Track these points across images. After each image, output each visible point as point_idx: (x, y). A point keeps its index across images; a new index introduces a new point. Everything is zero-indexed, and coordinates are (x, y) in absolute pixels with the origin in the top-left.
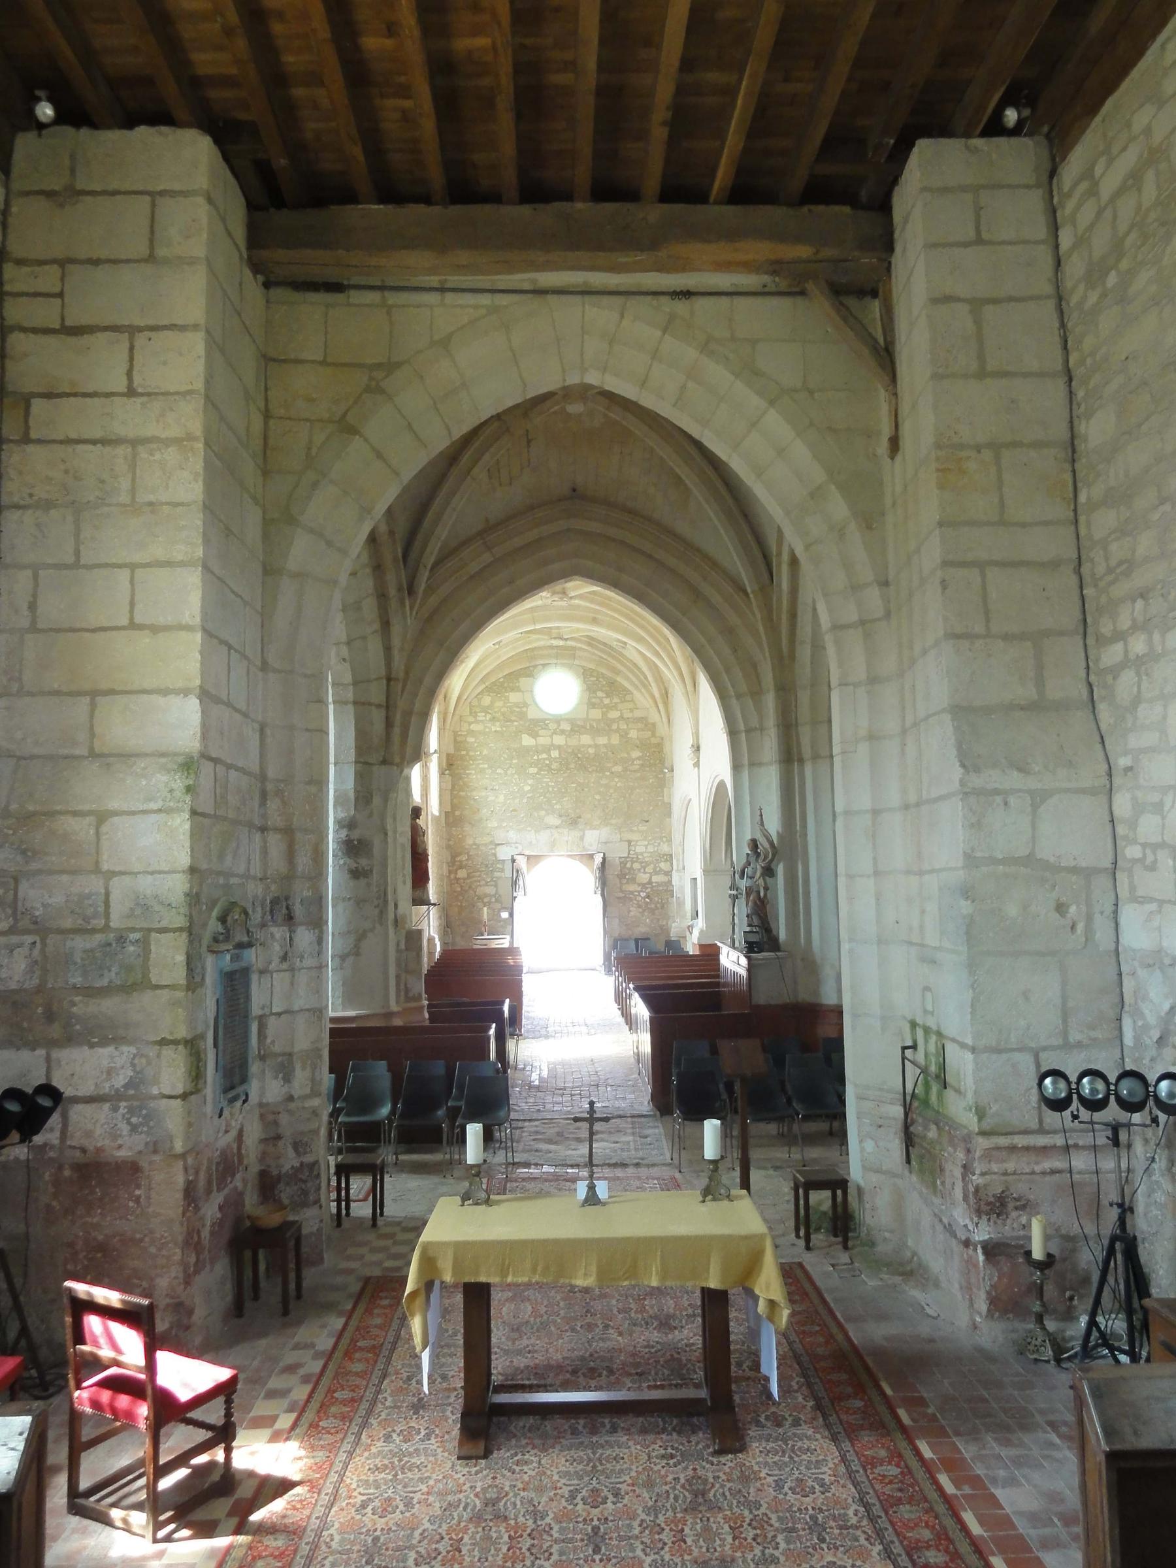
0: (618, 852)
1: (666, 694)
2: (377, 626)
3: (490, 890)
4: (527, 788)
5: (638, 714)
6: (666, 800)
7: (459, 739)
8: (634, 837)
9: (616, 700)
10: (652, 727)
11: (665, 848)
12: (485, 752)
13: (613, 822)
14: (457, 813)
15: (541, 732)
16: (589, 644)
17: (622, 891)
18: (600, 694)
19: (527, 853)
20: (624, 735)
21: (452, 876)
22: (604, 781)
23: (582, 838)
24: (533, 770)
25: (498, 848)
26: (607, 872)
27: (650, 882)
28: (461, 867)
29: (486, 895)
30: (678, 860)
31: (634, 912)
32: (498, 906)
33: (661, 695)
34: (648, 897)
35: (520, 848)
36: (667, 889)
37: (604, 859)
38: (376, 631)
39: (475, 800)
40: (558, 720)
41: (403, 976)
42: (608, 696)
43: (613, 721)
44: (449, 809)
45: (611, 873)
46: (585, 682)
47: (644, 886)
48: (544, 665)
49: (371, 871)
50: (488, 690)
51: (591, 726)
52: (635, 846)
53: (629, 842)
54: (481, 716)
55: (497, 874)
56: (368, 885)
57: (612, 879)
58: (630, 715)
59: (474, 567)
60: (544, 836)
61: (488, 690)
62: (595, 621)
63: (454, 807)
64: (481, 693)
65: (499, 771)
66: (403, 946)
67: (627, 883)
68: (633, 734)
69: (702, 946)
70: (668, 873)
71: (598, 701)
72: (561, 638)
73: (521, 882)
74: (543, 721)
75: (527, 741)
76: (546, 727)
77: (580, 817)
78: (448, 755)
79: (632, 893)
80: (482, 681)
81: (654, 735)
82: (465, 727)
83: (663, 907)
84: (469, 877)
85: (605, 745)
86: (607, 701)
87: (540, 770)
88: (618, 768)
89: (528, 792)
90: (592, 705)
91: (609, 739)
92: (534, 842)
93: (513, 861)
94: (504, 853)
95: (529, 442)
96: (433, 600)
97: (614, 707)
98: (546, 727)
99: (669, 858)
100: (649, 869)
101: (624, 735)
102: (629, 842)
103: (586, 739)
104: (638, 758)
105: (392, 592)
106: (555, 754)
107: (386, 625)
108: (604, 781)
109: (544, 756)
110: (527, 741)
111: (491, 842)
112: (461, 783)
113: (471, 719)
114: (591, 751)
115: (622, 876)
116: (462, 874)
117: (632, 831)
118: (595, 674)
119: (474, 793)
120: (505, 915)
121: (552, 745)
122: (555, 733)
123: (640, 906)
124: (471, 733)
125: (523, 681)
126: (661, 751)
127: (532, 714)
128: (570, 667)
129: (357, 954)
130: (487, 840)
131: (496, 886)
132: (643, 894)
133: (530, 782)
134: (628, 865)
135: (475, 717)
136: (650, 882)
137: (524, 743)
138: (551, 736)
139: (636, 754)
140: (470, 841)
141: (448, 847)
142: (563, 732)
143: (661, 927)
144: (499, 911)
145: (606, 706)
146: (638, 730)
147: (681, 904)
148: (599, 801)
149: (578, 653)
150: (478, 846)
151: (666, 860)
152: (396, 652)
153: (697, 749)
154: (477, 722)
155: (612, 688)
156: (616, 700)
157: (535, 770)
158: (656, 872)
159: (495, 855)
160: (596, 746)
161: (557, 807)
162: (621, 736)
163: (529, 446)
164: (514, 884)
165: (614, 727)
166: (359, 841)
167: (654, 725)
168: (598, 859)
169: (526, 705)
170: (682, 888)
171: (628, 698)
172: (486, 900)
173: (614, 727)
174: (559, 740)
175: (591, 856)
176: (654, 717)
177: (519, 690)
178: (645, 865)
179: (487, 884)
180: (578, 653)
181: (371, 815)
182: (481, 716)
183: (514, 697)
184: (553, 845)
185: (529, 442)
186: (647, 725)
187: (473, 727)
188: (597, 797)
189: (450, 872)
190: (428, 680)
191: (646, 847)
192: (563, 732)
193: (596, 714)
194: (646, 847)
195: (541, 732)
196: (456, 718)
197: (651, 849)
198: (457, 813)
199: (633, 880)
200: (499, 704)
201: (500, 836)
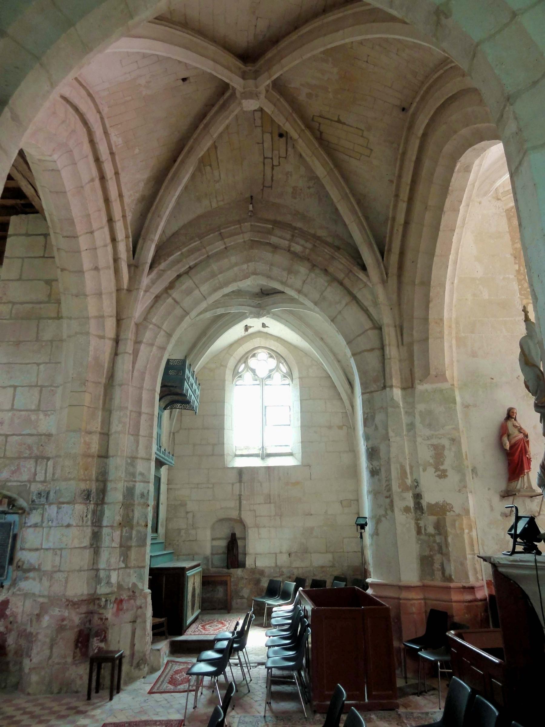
2: (347, 299)
38: (346, 305)
41: (438, 558)
49: (380, 469)
56: (379, 480)
59: (401, 218)
66: (431, 530)
95: (339, 121)
96: (394, 258)
105: (341, 276)
107: (354, 298)
129: (377, 534)
152: (371, 310)
163: (344, 124)
166: (372, 449)
181: (376, 428)
185: (339, 121)
190: (417, 313)
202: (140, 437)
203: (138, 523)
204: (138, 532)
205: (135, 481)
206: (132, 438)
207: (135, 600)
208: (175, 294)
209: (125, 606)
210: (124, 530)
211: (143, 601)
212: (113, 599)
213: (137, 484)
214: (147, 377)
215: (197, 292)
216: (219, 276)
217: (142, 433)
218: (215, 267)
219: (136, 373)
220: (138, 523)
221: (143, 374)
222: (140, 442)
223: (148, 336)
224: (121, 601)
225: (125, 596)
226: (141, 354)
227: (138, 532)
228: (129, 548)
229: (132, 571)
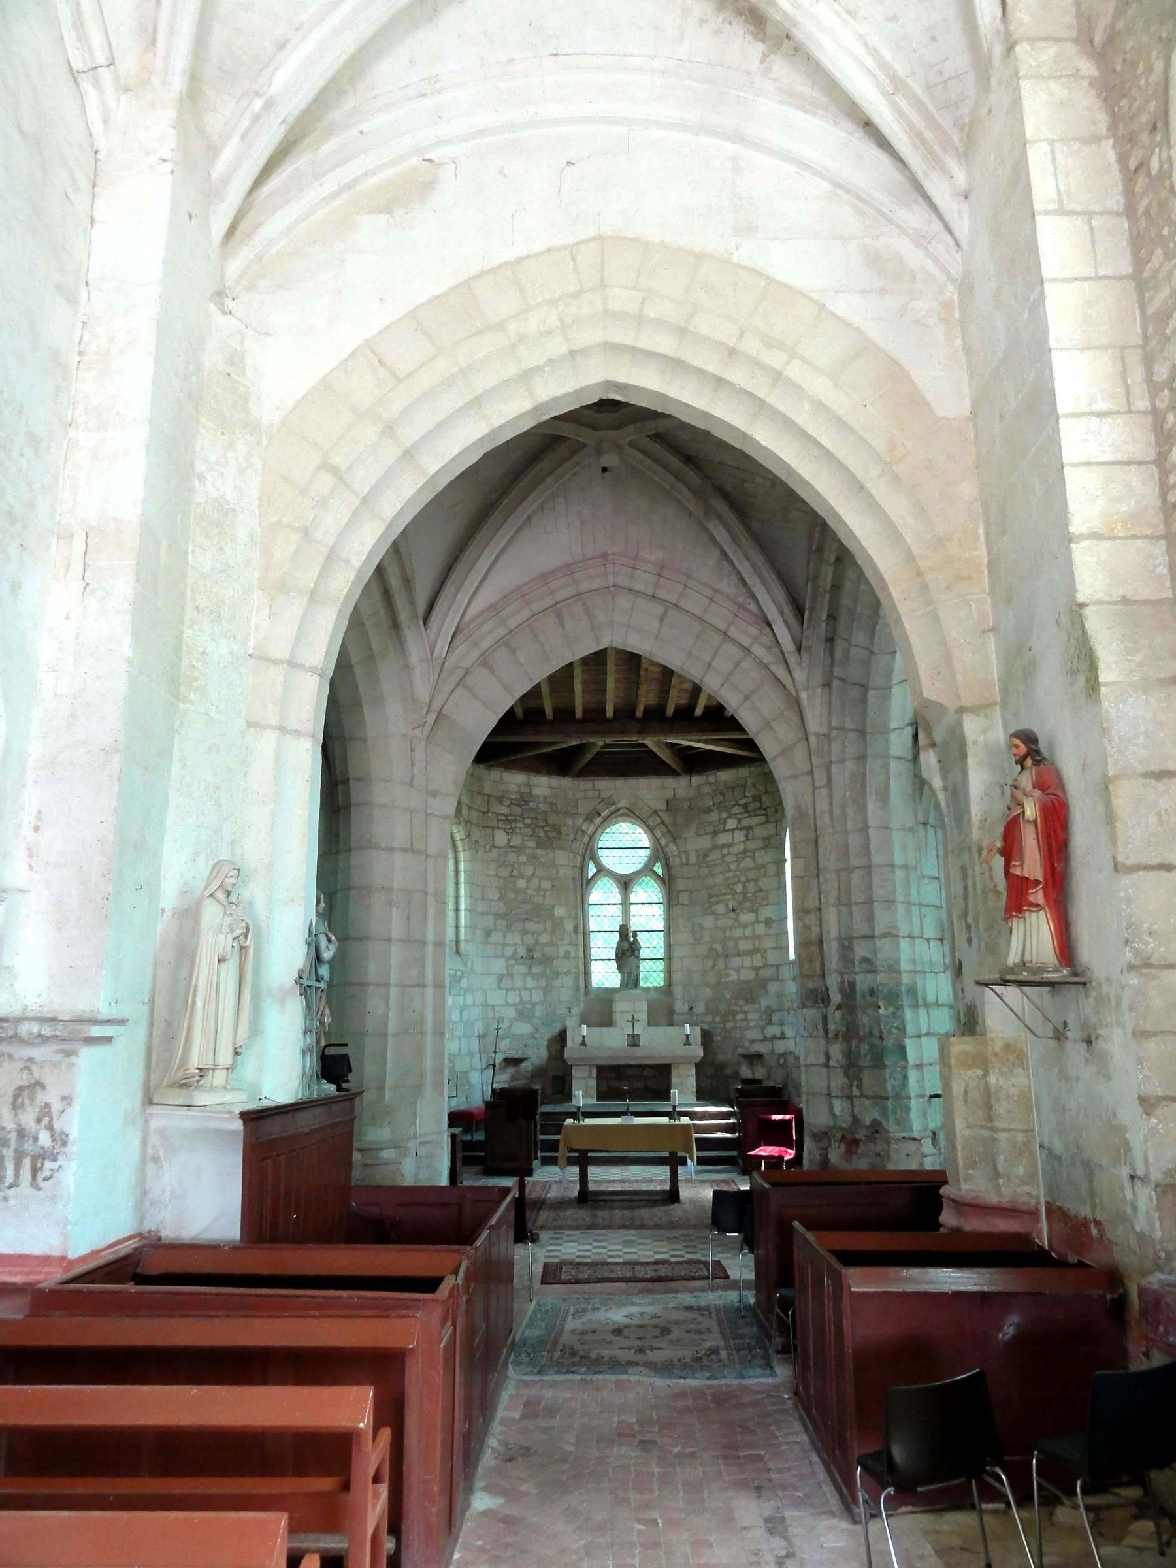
202: (854, 908)
203: (871, 1033)
204: (872, 1046)
205: (856, 973)
206: (844, 910)
207: (875, 1143)
208: (837, 671)
209: (862, 1148)
210: (854, 1043)
211: (886, 1147)
212: (839, 1135)
213: (859, 978)
214: (850, 812)
215: (854, 652)
216: (858, 611)
217: (857, 896)
218: (845, 601)
219: (837, 811)
220: (871, 1033)
221: (843, 807)
222: (855, 913)
223: (836, 748)
224: (856, 1142)
225: (861, 1135)
226: (834, 780)
227: (872, 1046)
228: (861, 1068)
229: (867, 1102)
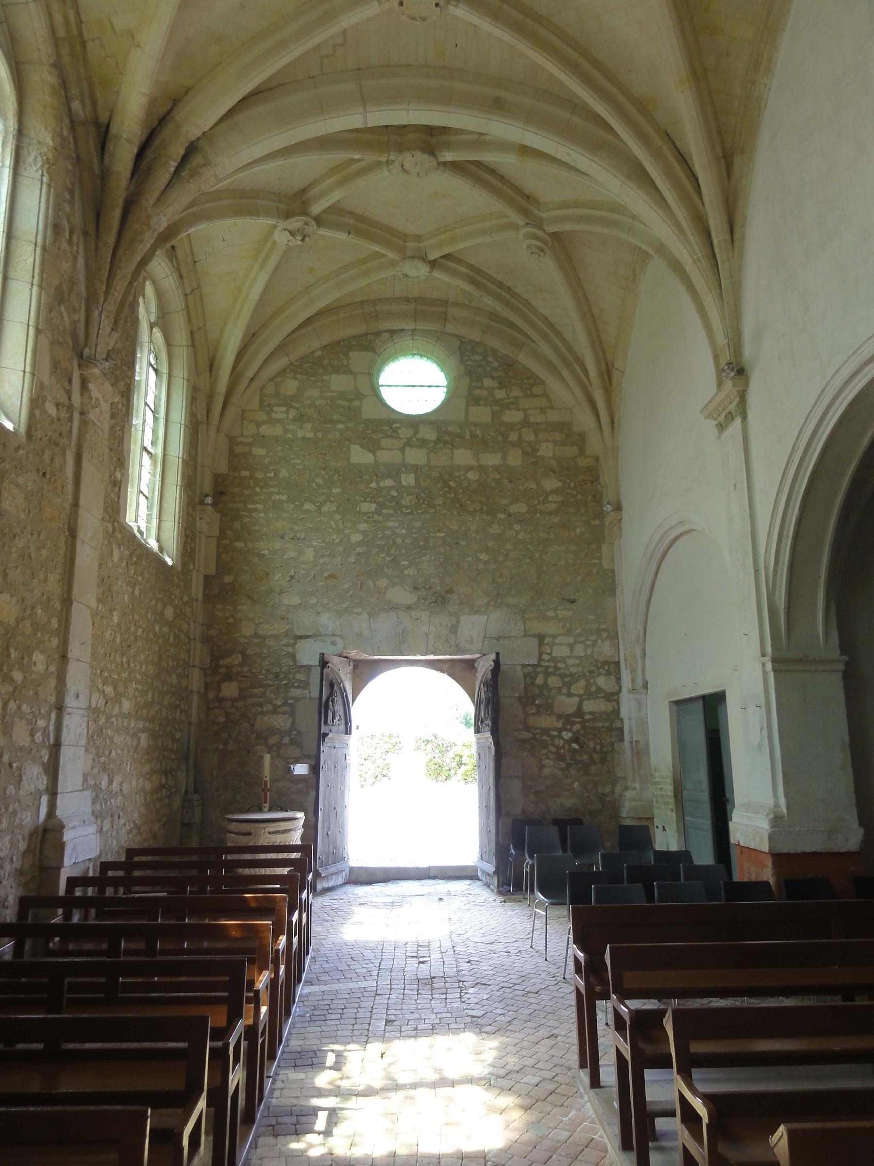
0: (521, 655)
1: (608, 374)
3: (281, 722)
4: (356, 538)
5: (553, 416)
6: (606, 565)
7: (238, 449)
8: (549, 628)
9: (516, 393)
10: (580, 441)
11: (606, 649)
12: (284, 473)
13: (511, 600)
14: (228, 579)
15: (385, 442)
16: (473, 282)
17: (527, 728)
18: (488, 382)
19: (353, 654)
20: (530, 451)
21: (211, 695)
22: (495, 530)
23: (454, 629)
24: (366, 507)
25: (301, 645)
26: (501, 692)
27: (579, 712)
28: (229, 677)
29: (273, 731)
30: (633, 671)
31: (550, 767)
32: (295, 752)
33: (601, 375)
34: (576, 740)
35: (340, 642)
36: (611, 726)
37: (497, 662)
39: (261, 557)
40: (415, 422)
42: (502, 386)
43: (511, 427)
44: (213, 571)
45: (508, 696)
46: (462, 362)
47: (568, 720)
48: (392, 332)
50: (294, 369)
51: (474, 436)
52: (553, 644)
53: (541, 638)
54: (279, 412)
55: (295, 692)
57: (506, 709)
58: (540, 418)
60: (386, 623)
61: (294, 369)
62: (498, 106)
63: (223, 567)
64: (283, 372)
65: (307, 506)
67: (538, 713)
68: (546, 450)
69: (779, 859)
70: (613, 697)
71: (484, 393)
72: (423, 258)
73: (339, 708)
74: (390, 422)
75: (359, 456)
76: (394, 434)
77: (450, 591)
78: (216, 476)
79: (546, 731)
80: (282, 347)
81: (582, 451)
82: (250, 429)
83: (603, 760)
84: (243, 695)
85: (496, 468)
86: (500, 394)
87: (381, 506)
88: (521, 508)
89: (358, 544)
90: (474, 400)
91: (504, 458)
92: (366, 634)
93: (324, 663)
94: (308, 654)
97: (514, 404)
98: (394, 434)
99: (613, 668)
100: (578, 688)
101: (530, 451)
102: (541, 638)
103: (463, 457)
104: (556, 492)
106: (408, 480)
108: (495, 530)
109: (389, 482)
110: (359, 456)
111: (287, 634)
112: (237, 525)
113: (262, 416)
114: (472, 476)
115: (526, 700)
116: (230, 690)
117: (546, 618)
118: (480, 349)
119: (261, 544)
120: (301, 769)
121: (404, 465)
122: (408, 444)
123: (560, 758)
124: (261, 440)
125: (356, 356)
126: (596, 479)
127: (368, 411)
128: (439, 337)
130: (283, 628)
131: (292, 714)
132: (567, 735)
133: (363, 526)
134: (539, 680)
135: (269, 413)
136: (579, 712)
137: (352, 461)
138: (402, 450)
139: (551, 483)
140: (247, 630)
141: (207, 640)
142: (423, 443)
143: (602, 797)
144: (297, 761)
145: (496, 402)
146: (555, 442)
147: (641, 752)
148: (487, 563)
149: (453, 311)
150: (264, 638)
151: (608, 673)
153: (739, 371)
154: (272, 422)
155: (510, 373)
156: (516, 393)
157: (373, 507)
158: (589, 694)
159: (293, 657)
160: (482, 469)
161: (411, 571)
162: (525, 453)
164: (324, 709)
165: (513, 437)
167: (582, 436)
168: (485, 666)
169: (359, 396)
170: (643, 723)
171: (536, 390)
172: (272, 741)
173: (513, 437)
174: (416, 456)
175: (470, 665)
176: (584, 420)
177: (349, 372)
178: (569, 680)
179: (275, 710)
180: (453, 311)
182: (279, 412)
183: (339, 383)
184: (402, 647)
186: (566, 432)
187: (264, 430)
188: (483, 557)
189: (207, 686)
191: (571, 646)
192: (423, 443)
193: (482, 414)
194: (571, 646)
195: (385, 442)
196: (232, 412)
197: (579, 650)
198: (228, 579)
199: (548, 708)
200: (313, 393)
201: (304, 621)
